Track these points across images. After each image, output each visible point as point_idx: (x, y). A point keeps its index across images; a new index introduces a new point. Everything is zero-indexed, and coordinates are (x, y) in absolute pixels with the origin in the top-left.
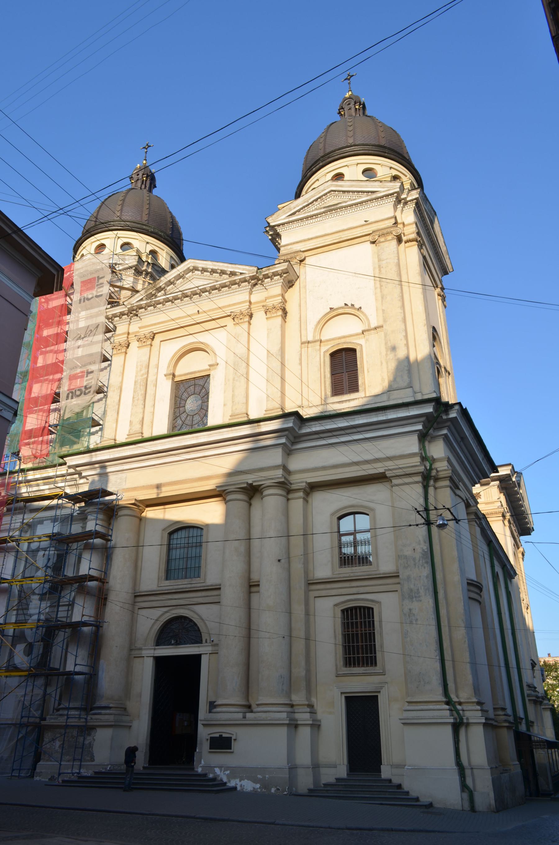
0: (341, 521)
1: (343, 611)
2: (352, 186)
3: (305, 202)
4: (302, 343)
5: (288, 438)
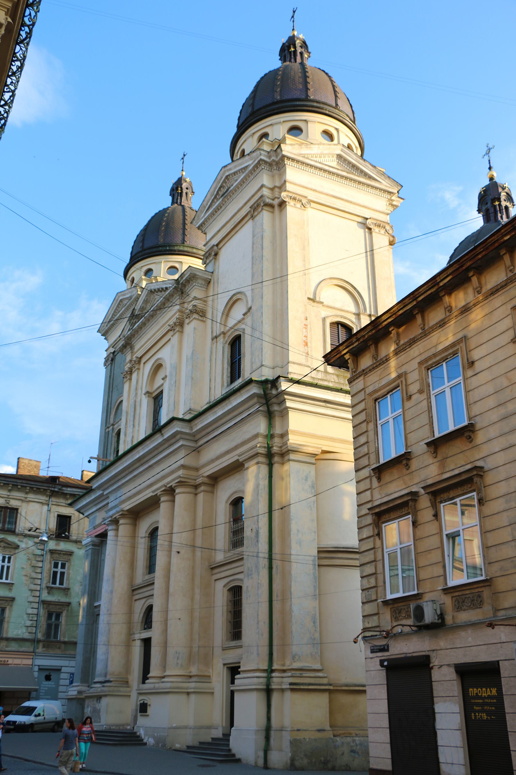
2: (235, 167)
3: (212, 196)
4: (213, 339)
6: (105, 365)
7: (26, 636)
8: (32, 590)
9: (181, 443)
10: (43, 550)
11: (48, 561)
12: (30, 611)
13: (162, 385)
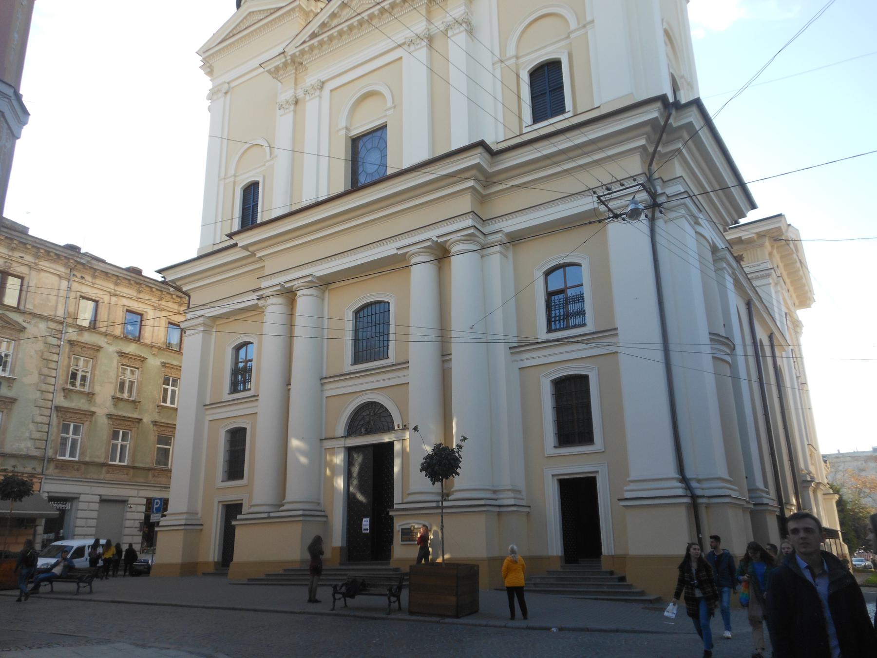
0: (549, 277)
1: (552, 381)
5: (477, 180)
6: (210, 97)
7: (34, 453)
8: (42, 392)
9: (471, 183)
10: (60, 339)
11: (66, 355)
12: (39, 419)
13: (386, 116)
